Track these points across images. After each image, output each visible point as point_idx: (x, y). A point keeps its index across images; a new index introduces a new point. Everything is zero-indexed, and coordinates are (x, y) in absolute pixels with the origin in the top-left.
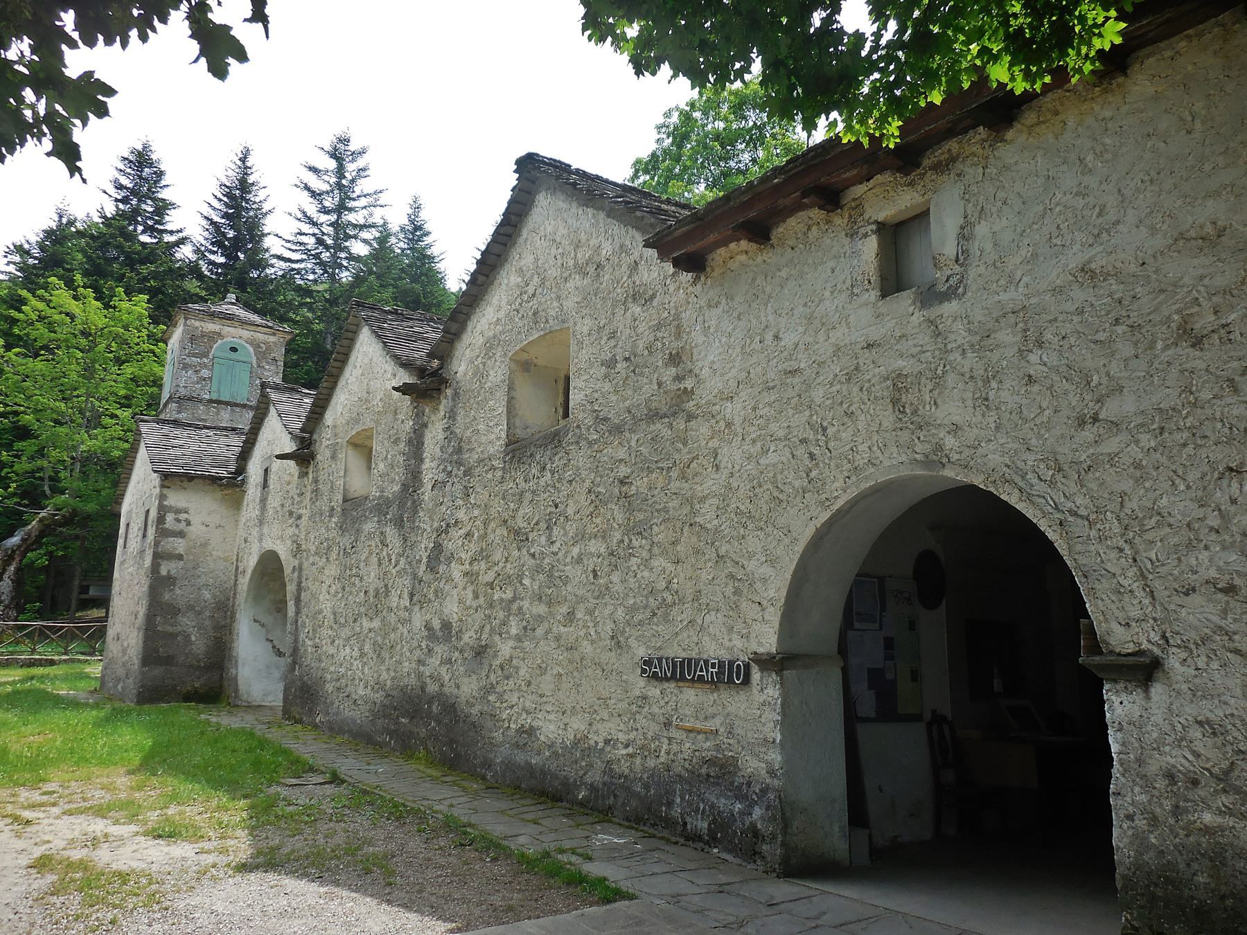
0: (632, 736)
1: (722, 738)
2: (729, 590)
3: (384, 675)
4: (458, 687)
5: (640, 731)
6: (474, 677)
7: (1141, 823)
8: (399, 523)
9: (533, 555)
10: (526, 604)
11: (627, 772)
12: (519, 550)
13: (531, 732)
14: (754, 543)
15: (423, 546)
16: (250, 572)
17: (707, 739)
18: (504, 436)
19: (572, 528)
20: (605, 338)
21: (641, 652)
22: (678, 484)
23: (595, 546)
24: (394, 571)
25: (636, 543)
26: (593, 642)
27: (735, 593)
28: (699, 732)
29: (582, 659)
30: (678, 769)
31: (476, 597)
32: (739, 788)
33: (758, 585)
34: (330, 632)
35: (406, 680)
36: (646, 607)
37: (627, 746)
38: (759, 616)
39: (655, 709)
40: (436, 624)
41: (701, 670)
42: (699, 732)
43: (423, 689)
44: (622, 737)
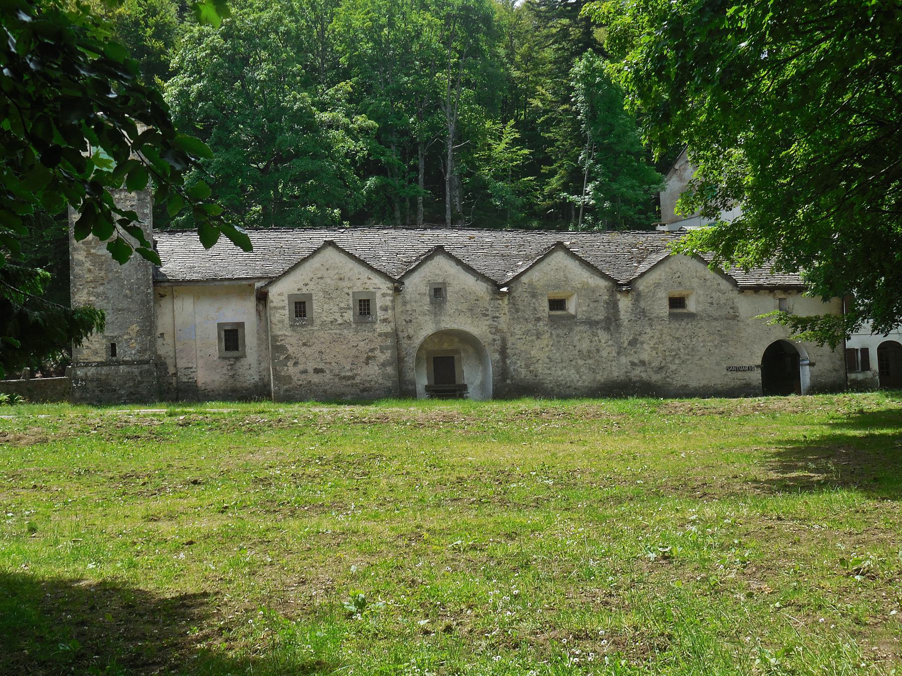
3: (598, 377)
8: (607, 329)
10: (682, 356)
13: (687, 385)
14: (756, 346)
16: (422, 338)
19: (700, 340)
21: (725, 366)
24: (604, 345)
31: (657, 353)
34: (546, 365)
35: (616, 378)
40: (636, 361)
43: (630, 380)
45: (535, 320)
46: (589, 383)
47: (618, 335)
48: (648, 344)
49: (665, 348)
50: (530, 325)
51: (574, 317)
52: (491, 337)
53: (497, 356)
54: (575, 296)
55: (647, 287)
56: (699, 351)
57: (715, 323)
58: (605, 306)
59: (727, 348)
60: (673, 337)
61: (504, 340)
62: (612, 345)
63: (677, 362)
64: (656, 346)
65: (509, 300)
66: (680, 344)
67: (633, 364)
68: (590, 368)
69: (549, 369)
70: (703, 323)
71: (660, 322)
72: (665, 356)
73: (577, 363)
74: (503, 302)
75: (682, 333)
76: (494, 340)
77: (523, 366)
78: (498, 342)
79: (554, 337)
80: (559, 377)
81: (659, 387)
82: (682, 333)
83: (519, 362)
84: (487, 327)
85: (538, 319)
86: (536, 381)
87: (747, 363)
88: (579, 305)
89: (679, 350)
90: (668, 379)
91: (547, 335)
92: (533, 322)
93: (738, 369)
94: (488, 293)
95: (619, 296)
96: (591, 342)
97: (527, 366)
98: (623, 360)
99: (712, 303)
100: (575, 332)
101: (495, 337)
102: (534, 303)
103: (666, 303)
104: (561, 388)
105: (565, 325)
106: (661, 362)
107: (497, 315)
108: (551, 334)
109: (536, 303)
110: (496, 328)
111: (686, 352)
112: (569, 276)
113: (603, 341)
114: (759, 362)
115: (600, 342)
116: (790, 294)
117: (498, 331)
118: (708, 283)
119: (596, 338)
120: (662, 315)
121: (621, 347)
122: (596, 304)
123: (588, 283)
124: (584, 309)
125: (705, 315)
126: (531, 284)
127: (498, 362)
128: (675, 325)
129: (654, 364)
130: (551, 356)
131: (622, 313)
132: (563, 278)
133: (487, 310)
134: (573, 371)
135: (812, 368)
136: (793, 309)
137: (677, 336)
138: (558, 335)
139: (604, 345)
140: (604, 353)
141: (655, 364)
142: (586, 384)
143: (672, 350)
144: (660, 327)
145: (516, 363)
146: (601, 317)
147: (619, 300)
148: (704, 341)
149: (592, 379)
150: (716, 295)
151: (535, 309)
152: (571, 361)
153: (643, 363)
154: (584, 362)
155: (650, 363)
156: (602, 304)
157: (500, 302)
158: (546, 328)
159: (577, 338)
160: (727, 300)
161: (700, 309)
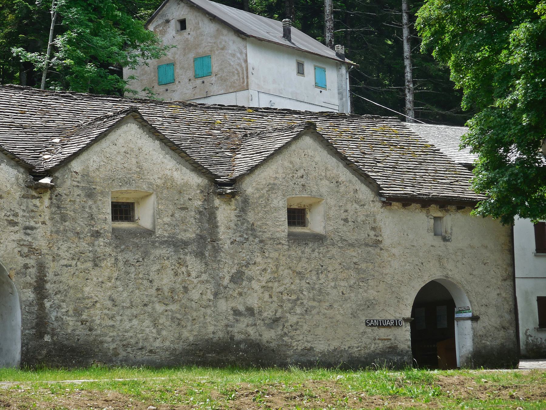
0: (360, 344)
1: (393, 341)
2: (396, 301)
3: (186, 334)
4: (261, 335)
5: (364, 342)
6: (273, 331)
7: (477, 344)
8: (200, 255)
9: (309, 283)
10: (305, 302)
11: (357, 356)
12: (300, 280)
13: (311, 349)
15: (225, 270)
18: (286, 231)
19: (331, 276)
20: (342, 211)
21: (363, 319)
22: (377, 268)
23: (343, 283)
24: (195, 281)
25: (361, 284)
30: (378, 351)
31: (271, 297)
32: (398, 353)
33: (405, 300)
34: (106, 311)
35: (211, 336)
36: (365, 304)
37: (358, 348)
39: (370, 335)
40: (241, 308)
43: (232, 338)
44: (356, 345)
45: (92, 236)
46: (172, 342)
47: (215, 266)
48: (259, 280)
49: (282, 289)
50: (84, 244)
51: (150, 233)
52: (21, 261)
53: (30, 295)
54: (153, 198)
55: (257, 189)
56: (328, 294)
57: (351, 252)
58: (198, 216)
59: (366, 291)
60: (294, 271)
61: (41, 267)
62: (207, 281)
63: (298, 310)
64: (270, 284)
65: (51, 199)
66: (304, 281)
67: (236, 312)
68: (173, 318)
69: (112, 318)
70: (334, 251)
71: (276, 247)
72: (282, 301)
73: (154, 309)
74: (41, 203)
75: (306, 266)
76: (26, 267)
77: (71, 312)
78: (33, 271)
79: (121, 264)
80: (127, 331)
81: (273, 351)
82: (306, 266)
83: (64, 305)
84: (15, 245)
85: (97, 234)
86: (92, 338)
87: (390, 315)
88: (157, 214)
89: (301, 291)
90: (285, 339)
91: (109, 262)
92: (88, 239)
93: (381, 324)
94: (18, 185)
95: (217, 202)
96: (176, 274)
97: (78, 312)
98: (223, 305)
99: (346, 220)
100: (152, 257)
101: (27, 261)
102: (90, 207)
103: (284, 216)
104: (129, 350)
105: (137, 246)
106: (276, 311)
107: (32, 224)
108: (116, 259)
109: (94, 206)
110: (30, 246)
111: (311, 295)
112: (145, 165)
113: (194, 274)
114: (408, 313)
115: (189, 275)
116: (447, 211)
117: (32, 250)
118: (342, 189)
119: (184, 269)
120: (278, 235)
121: (219, 285)
122: (183, 213)
123: (172, 179)
124: (167, 220)
125: (337, 238)
126: (86, 175)
127: (31, 305)
128: (296, 251)
129: (265, 314)
130: (115, 296)
131: (222, 229)
132: (134, 168)
133: (16, 215)
134: (147, 322)
135: (475, 324)
136: (451, 234)
137: (299, 269)
138: (126, 262)
139: (195, 281)
140: (195, 294)
141: (268, 314)
142: (167, 344)
143: (290, 293)
144: (275, 255)
145: (59, 307)
146: (190, 235)
147: (217, 208)
148: (335, 279)
149: (177, 335)
150: (352, 207)
151: (91, 217)
152: (145, 305)
153: (250, 311)
154: (163, 308)
155: (260, 312)
156: (193, 213)
157: (37, 202)
158: (108, 250)
159: (155, 268)
160: (367, 216)
161: (331, 228)
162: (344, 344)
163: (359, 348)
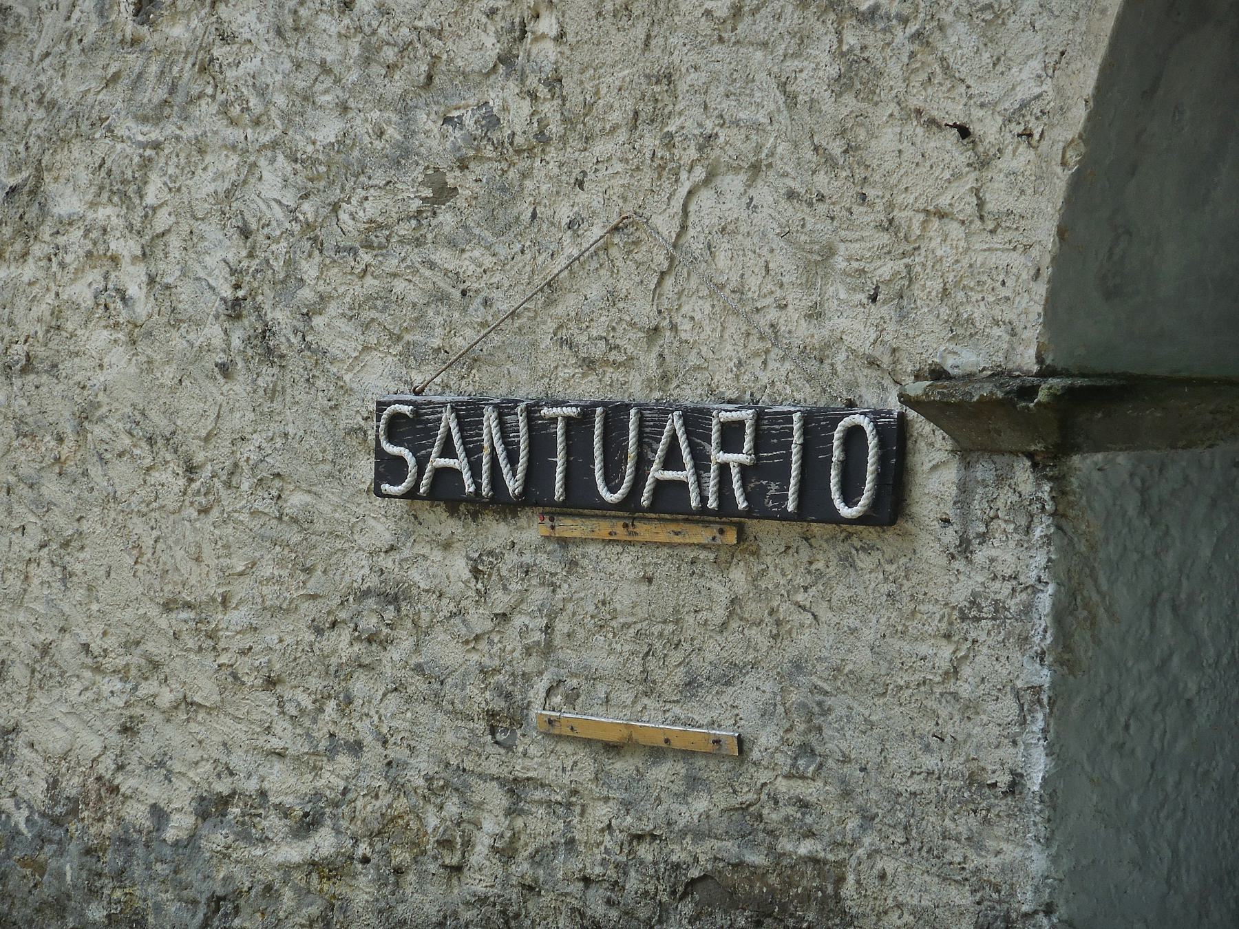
0: (332, 777)
5: (373, 754)
17: (694, 783)
26: (136, 334)
27: (841, 84)
28: (657, 752)
29: (84, 417)
36: (401, 157)
37: (307, 825)
38: (958, 197)
41: (672, 460)
42: (657, 752)
162: (148, 744)
163: (324, 842)
